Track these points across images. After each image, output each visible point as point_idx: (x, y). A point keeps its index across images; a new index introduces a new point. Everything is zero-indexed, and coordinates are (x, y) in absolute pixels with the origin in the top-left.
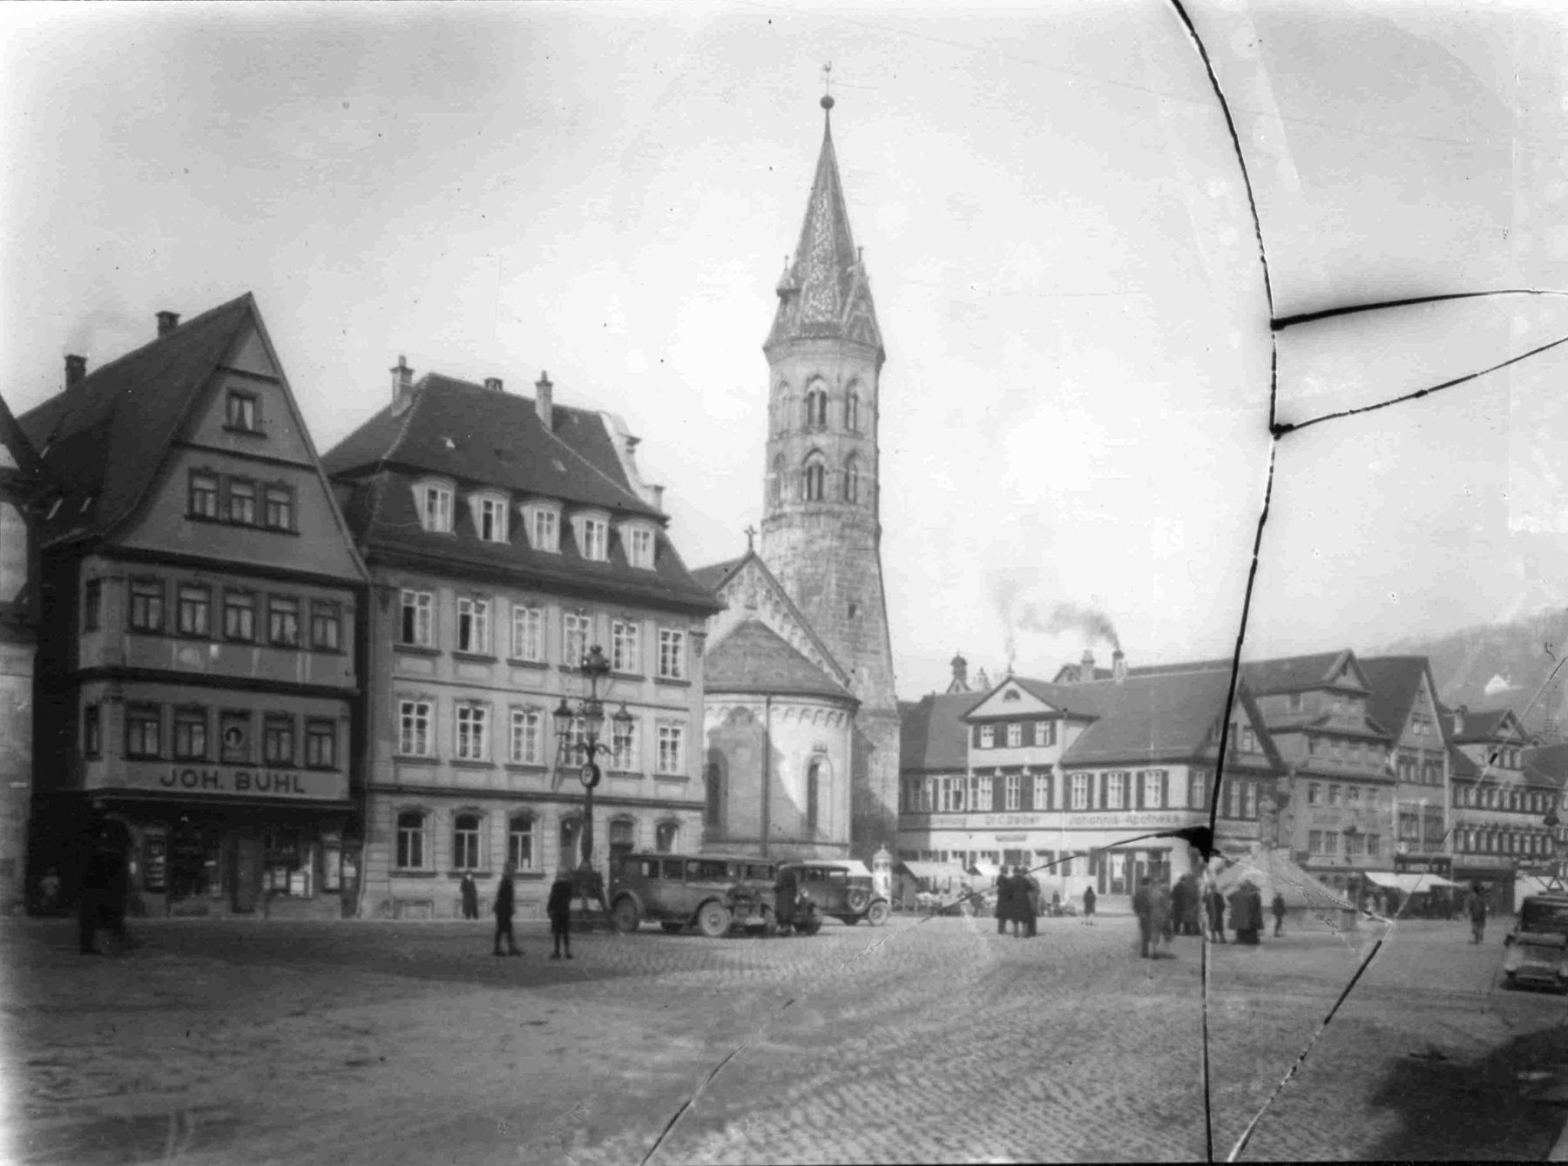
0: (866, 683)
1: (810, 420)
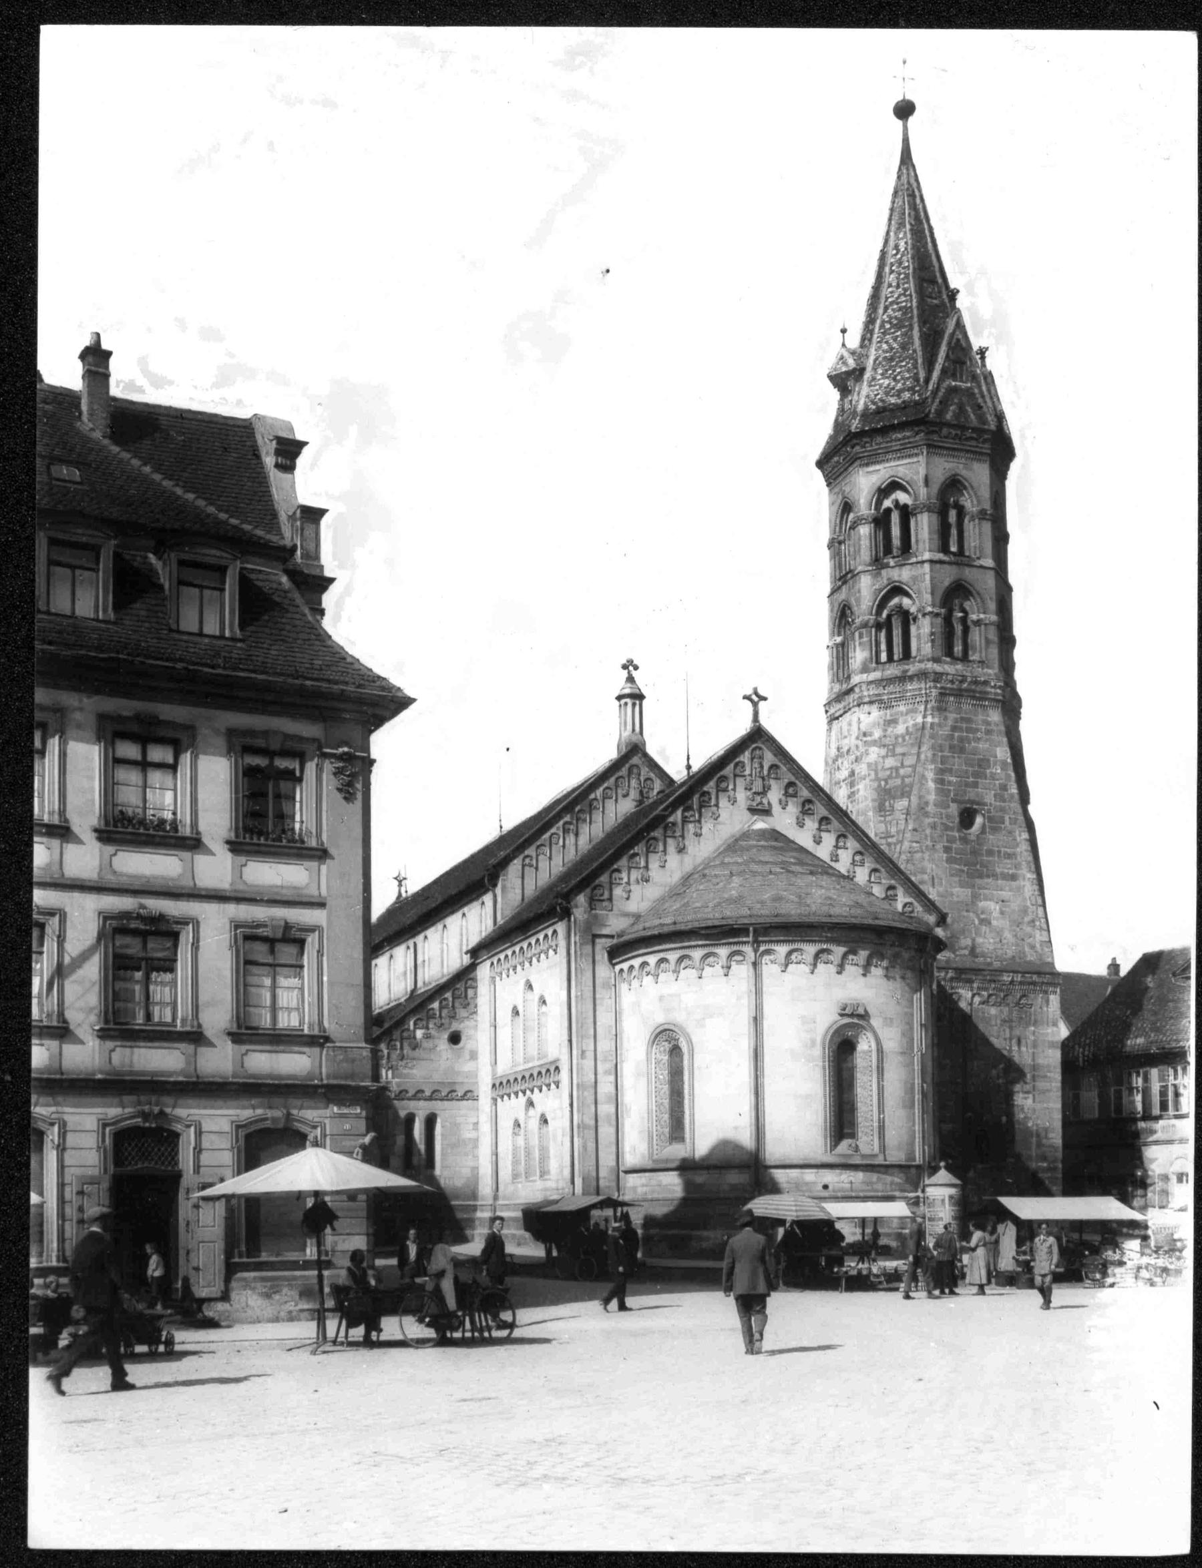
0: (994, 923)
1: (888, 550)
